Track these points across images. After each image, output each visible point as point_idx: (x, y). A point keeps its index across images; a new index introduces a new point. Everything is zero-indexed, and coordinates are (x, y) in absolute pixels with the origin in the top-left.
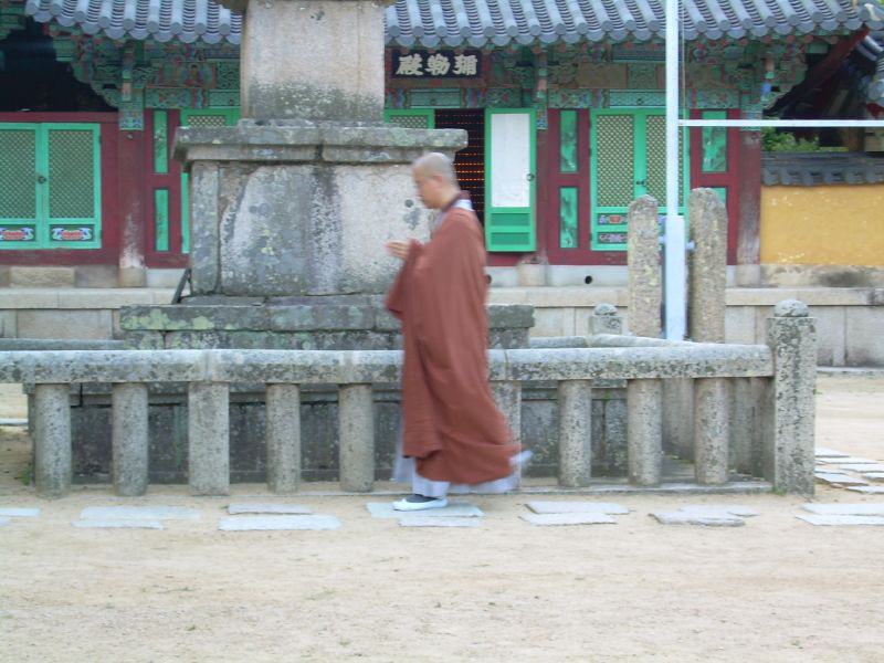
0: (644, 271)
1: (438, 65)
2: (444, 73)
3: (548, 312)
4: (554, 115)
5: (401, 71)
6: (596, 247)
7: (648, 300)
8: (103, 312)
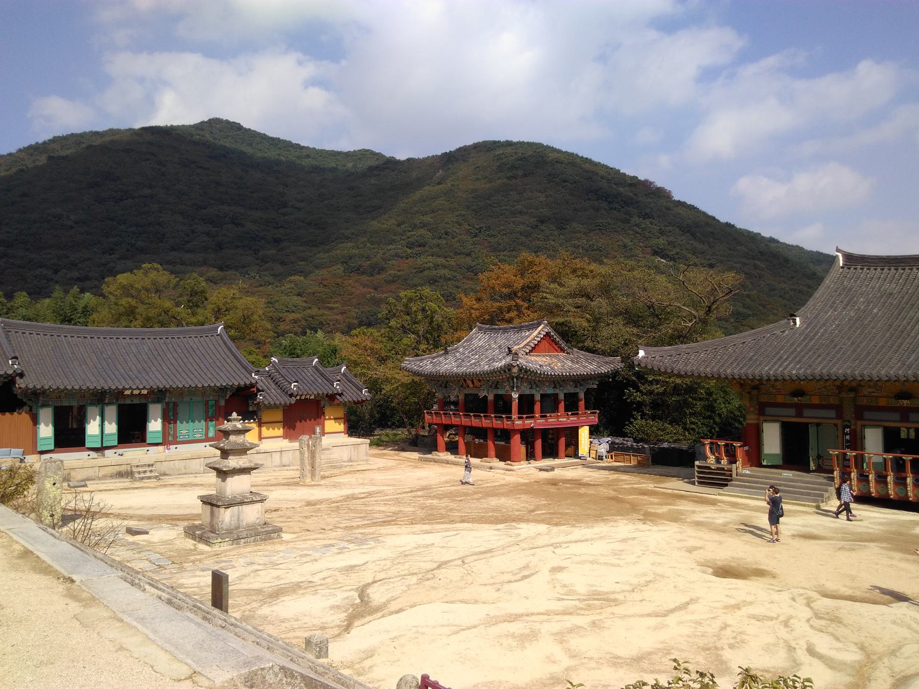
1: (136, 392)
4: (167, 404)
6: (178, 440)
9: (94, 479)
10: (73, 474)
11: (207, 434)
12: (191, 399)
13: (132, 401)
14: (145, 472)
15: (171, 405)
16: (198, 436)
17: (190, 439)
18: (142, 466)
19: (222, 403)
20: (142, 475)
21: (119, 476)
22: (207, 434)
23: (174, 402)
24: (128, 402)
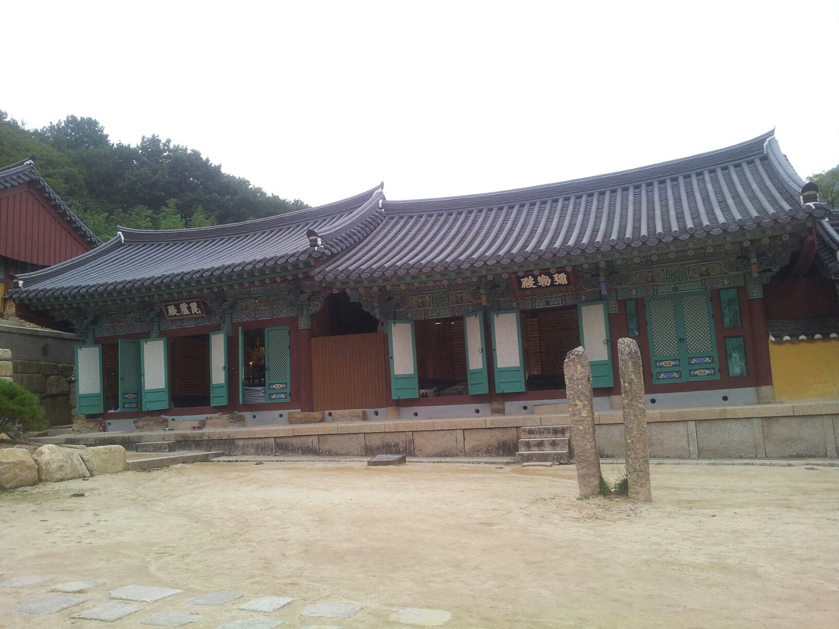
0: (576, 405)
1: (544, 281)
2: (549, 284)
3: (615, 426)
4: (622, 303)
5: (523, 286)
7: (581, 428)
8: (359, 435)
9: (457, 455)
10: (419, 440)
11: (724, 368)
12: (676, 289)
13: (548, 303)
14: (540, 444)
15: (631, 306)
16: (702, 373)
17: (685, 379)
18: (541, 432)
19: (756, 293)
20: (535, 451)
21: (503, 451)
22: (724, 368)
23: (636, 299)
24: (540, 305)
